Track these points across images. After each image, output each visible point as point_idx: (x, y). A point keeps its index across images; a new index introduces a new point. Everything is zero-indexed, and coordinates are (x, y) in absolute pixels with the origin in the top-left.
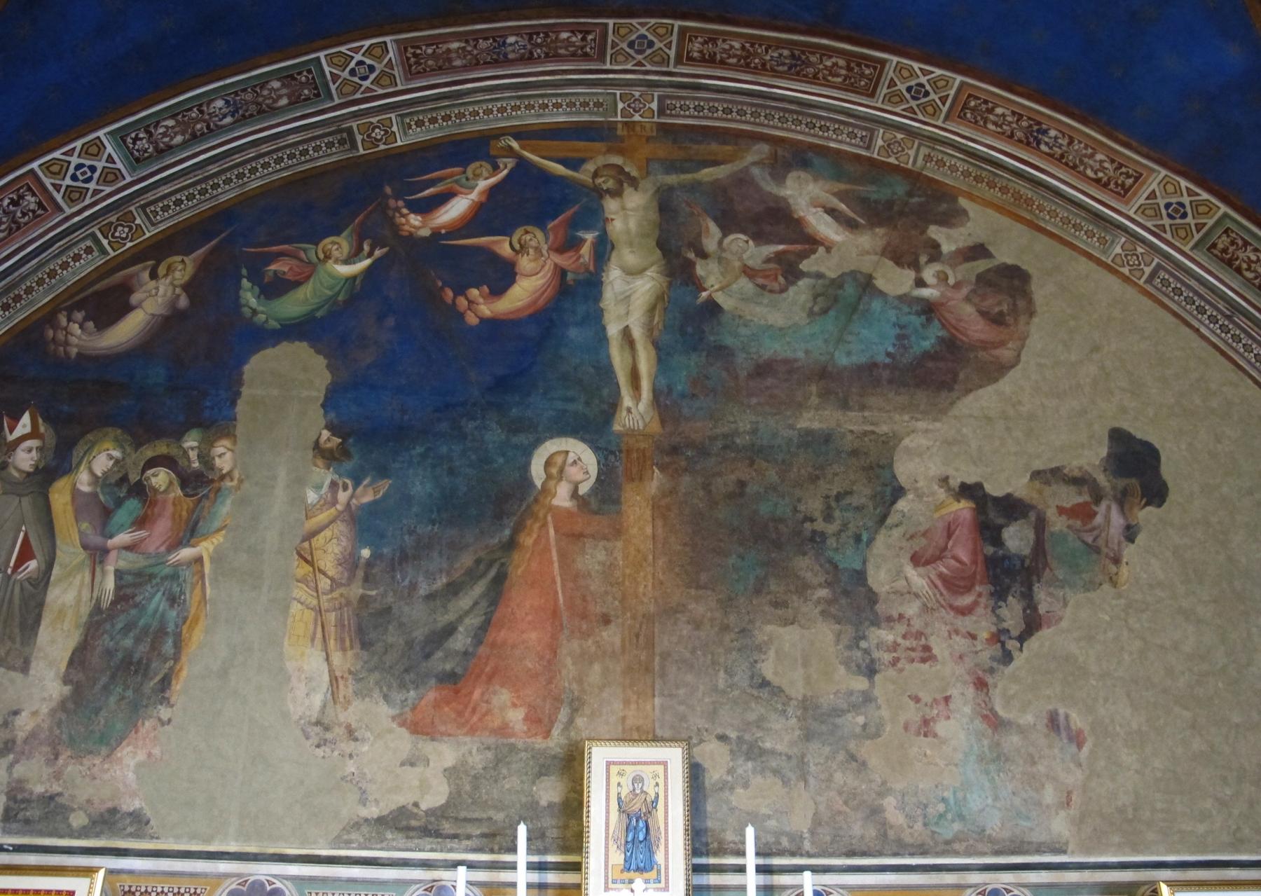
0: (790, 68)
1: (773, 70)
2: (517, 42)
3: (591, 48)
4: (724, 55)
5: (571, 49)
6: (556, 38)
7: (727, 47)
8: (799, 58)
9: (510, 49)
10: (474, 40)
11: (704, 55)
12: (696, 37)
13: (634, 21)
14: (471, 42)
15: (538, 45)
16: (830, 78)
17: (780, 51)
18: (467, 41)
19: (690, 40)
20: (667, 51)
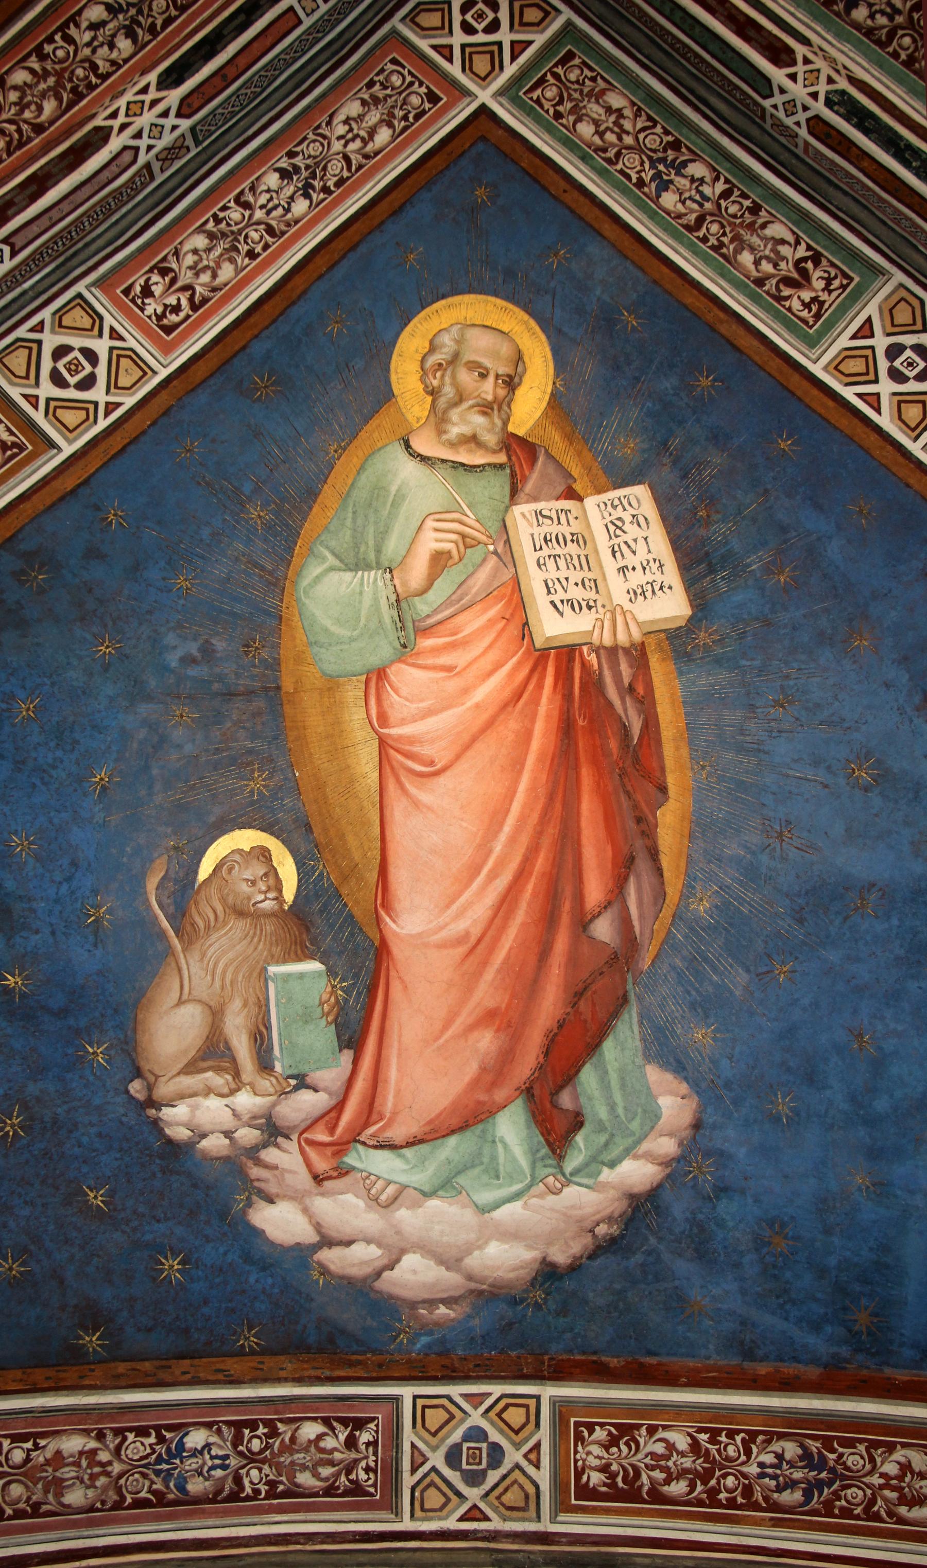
0: (808, 1495)
1: (775, 1507)
2: (208, 1446)
3: (367, 1470)
4: (659, 1475)
5: (326, 1471)
6: (293, 1439)
7: (660, 1448)
8: (822, 1464)
9: (192, 1464)
10: (118, 1432)
11: (613, 1476)
12: (591, 1427)
13: (456, 1390)
14: (110, 1436)
15: (252, 1458)
16: (903, 1510)
17: (776, 1446)
18: (101, 1436)
19: (579, 1438)
20: (531, 1470)
